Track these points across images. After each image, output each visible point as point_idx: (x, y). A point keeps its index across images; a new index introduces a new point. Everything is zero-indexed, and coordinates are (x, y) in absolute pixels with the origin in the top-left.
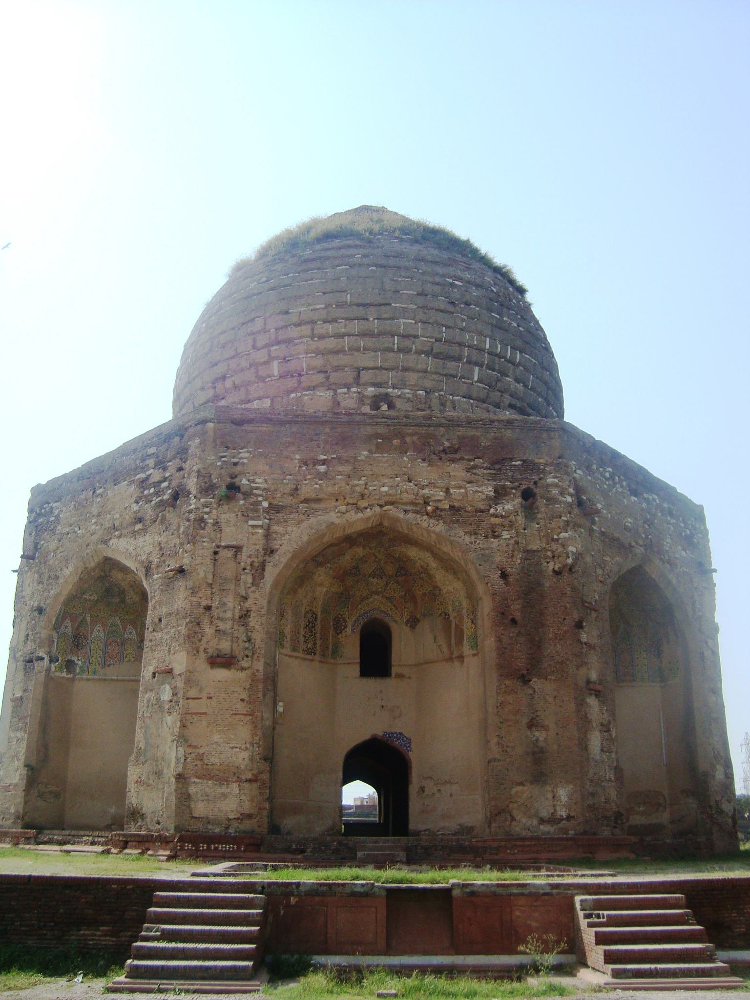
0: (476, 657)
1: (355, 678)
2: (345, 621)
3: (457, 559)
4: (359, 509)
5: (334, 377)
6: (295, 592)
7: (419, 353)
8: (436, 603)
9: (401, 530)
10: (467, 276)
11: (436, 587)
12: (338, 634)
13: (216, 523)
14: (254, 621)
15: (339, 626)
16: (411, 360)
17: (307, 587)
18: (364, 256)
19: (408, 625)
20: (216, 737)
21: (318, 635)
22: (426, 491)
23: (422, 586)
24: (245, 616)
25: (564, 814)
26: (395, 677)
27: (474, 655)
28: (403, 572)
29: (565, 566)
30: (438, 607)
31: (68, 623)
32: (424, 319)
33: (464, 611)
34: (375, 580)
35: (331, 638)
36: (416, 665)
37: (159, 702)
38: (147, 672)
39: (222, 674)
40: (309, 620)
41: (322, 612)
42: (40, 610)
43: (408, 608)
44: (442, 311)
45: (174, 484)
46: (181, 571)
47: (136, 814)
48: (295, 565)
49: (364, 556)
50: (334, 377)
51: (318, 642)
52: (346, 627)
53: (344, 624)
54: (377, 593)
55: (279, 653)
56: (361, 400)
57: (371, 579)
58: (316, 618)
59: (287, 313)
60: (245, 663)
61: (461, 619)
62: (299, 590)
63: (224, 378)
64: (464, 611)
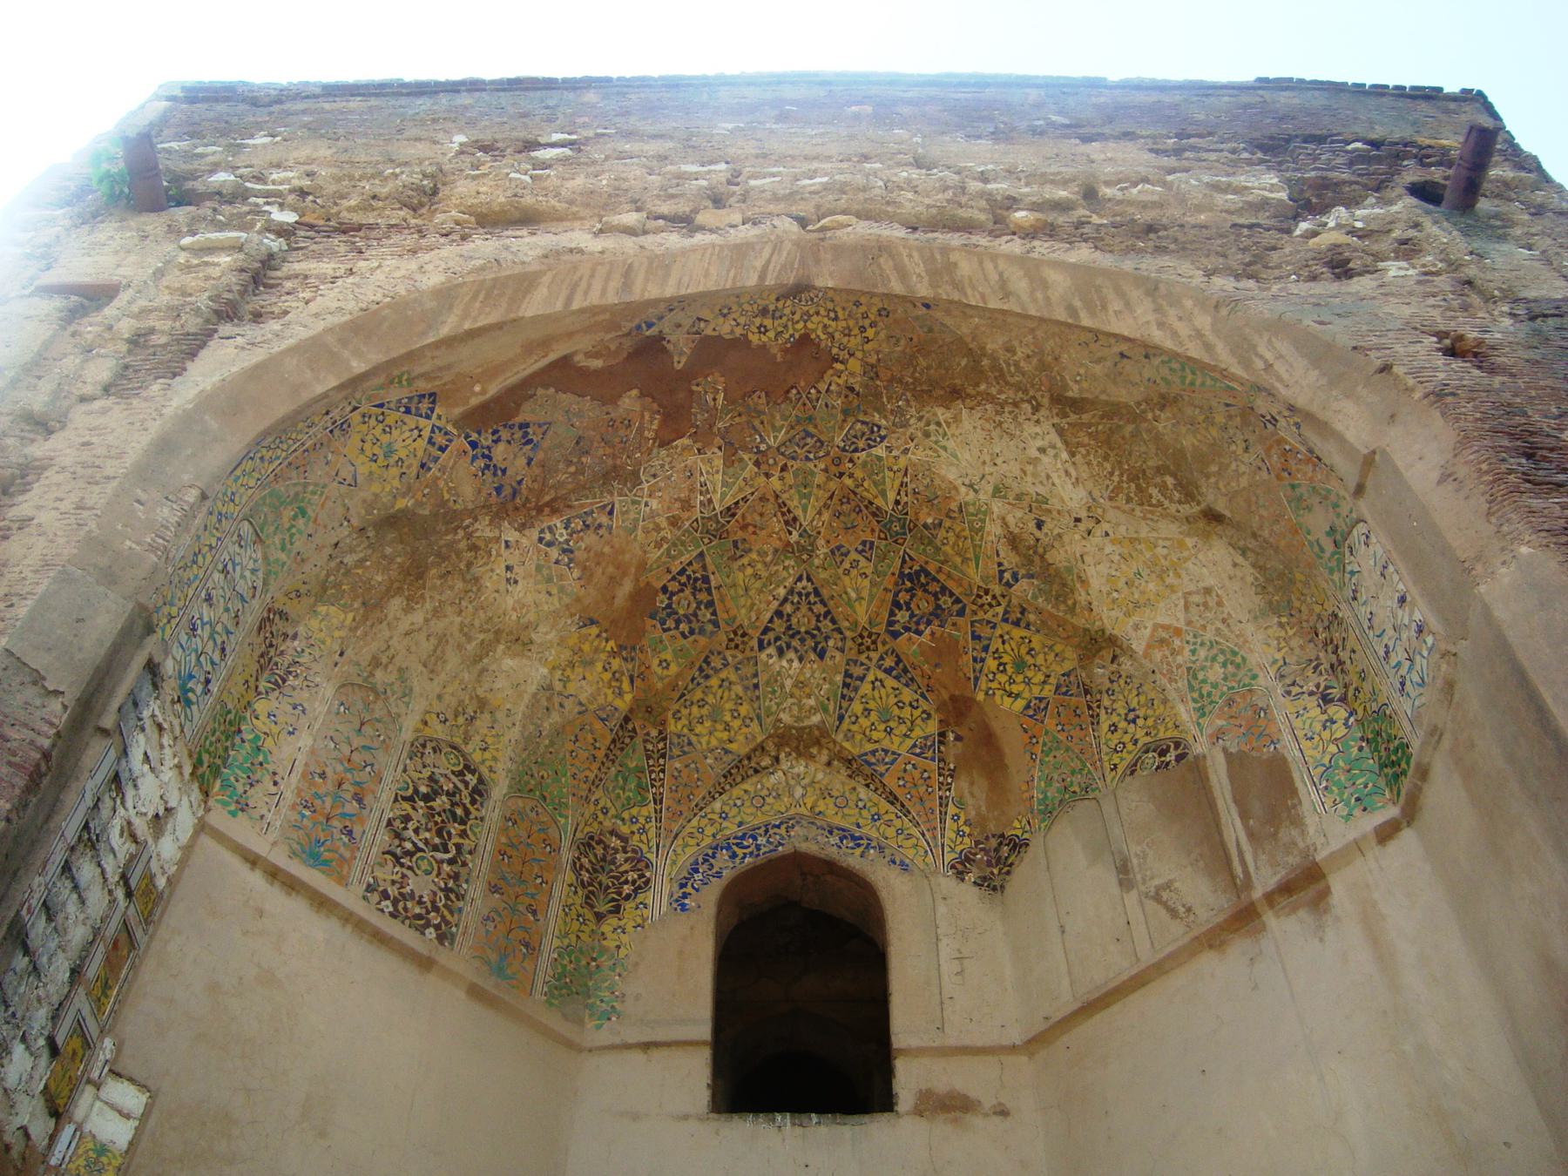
0: (1407, 836)
1: (686, 1117)
2: (639, 862)
3: (1194, 351)
6: (372, 607)
8: (1105, 727)
9: (897, 287)
11: (1099, 644)
12: (599, 917)
17: (437, 613)
19: (971, 877)
21: (480, 867)
23: (1020, 666)
26: (918, 1112)
27: (1386, 833)
28: (923, 605)
30: (1115, 739)
33: (1266, 680)
34: (790, 666)
35: (555, 908)
36: (1036, 1043)
40: (431, 778)
41: (520, 787)
43: (960, 804)
48: (358, 366)
49: (730, 512)
51: (475, 890)
52: (643, 885)
53: (632, 876)
54: (800, 741)
55: (202, 827)
57: (768, 656)
58: (479, 793)
61: (1258, 719)
62: (396, 604)
64: (1266, 680)
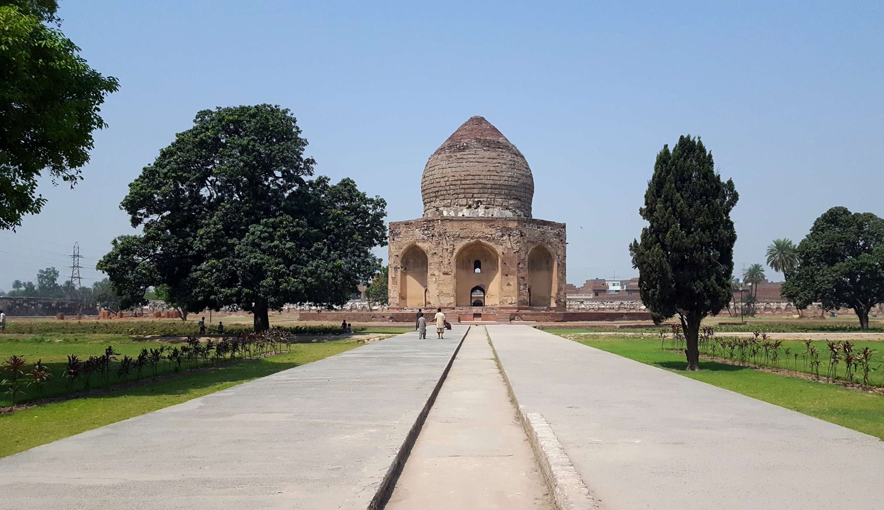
4: (472, 239)
5: (467, 195)
7: (489, 189)
10: (502, 161)
13: (442, 243)
14: (451, 264)
15: (469, 261)
16: (486, 190)
18: (474, 158)
20: (445, 288)
22: (487, 235)
24: (450, 263)
25: (513, 302)
29: (516, 252)
31: (404, 259)
32: (490, 178)
37: (432, 281)
38: (429, 274)
39: (446, 276)
42: (397, 256)
44: (495, 176)
45: (432, 233)
46: (435, 253)
47: (429, 303)
50: (467, 195)
56: (474, 202)
59: (454, 176)
60: (450, 273)
63: (438, 192)
